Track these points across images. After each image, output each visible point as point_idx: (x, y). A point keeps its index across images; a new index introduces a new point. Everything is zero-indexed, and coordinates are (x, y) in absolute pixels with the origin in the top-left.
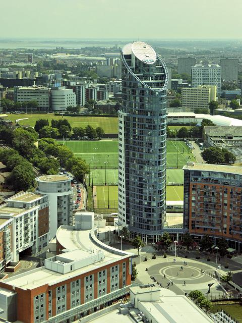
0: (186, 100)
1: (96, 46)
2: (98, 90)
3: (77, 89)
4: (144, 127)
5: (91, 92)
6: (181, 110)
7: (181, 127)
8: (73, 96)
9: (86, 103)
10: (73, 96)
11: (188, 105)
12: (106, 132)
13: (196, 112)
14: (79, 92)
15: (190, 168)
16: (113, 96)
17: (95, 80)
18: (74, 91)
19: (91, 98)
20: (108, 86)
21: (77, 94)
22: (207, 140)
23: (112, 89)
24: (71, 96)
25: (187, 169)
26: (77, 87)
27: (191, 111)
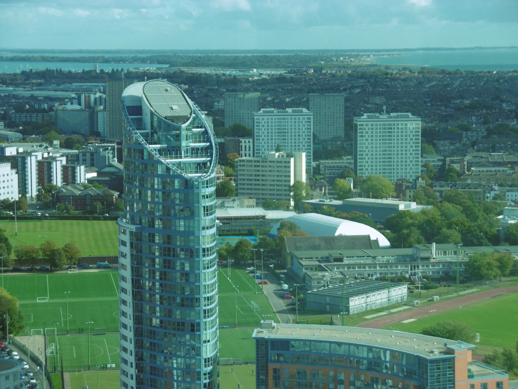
0: (246, 182)
1: (53, 66)
2: (64, 163)
3: (20, 164)
4: (172, 253)
5: (50, 168)
6: (237, 203)
7: (241, 238)
8: (9, 178)
9: (39, 190)
10: (9, 178)
11: (249, 191)
12: (85, 253)
13: (267, 206)
14: (24, 168)
15: (266, 334)
16: (95, 174)
17: (56, 142)
18: (12, 167)
19: (50, 180)
20: (84, 155)
21: (20, 172)
22: (292, 264)
23: (92, 160)
24: (6, 178)
25: (260, 335)
26: (20, 159)
27: (257, 204)
